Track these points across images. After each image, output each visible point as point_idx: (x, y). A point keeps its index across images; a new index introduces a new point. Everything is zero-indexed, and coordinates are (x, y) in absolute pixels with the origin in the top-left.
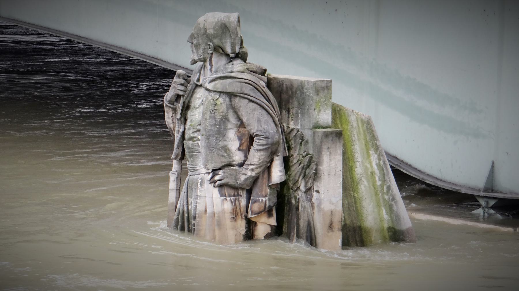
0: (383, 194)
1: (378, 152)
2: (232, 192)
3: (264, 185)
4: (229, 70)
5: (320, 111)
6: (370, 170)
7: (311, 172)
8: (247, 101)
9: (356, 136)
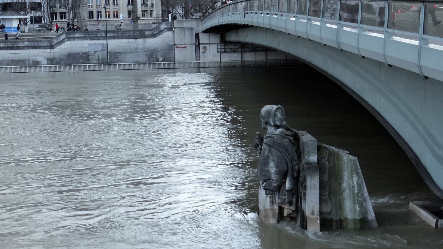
0: (358, 197)
1: (358, 176)
2: (271, 193)
3: (284, 191)
4: (273, 134)
5: (310, 155)
6: (352, 185)
7: (304, 185)
8: (274, 149)
9: (346, 167)
